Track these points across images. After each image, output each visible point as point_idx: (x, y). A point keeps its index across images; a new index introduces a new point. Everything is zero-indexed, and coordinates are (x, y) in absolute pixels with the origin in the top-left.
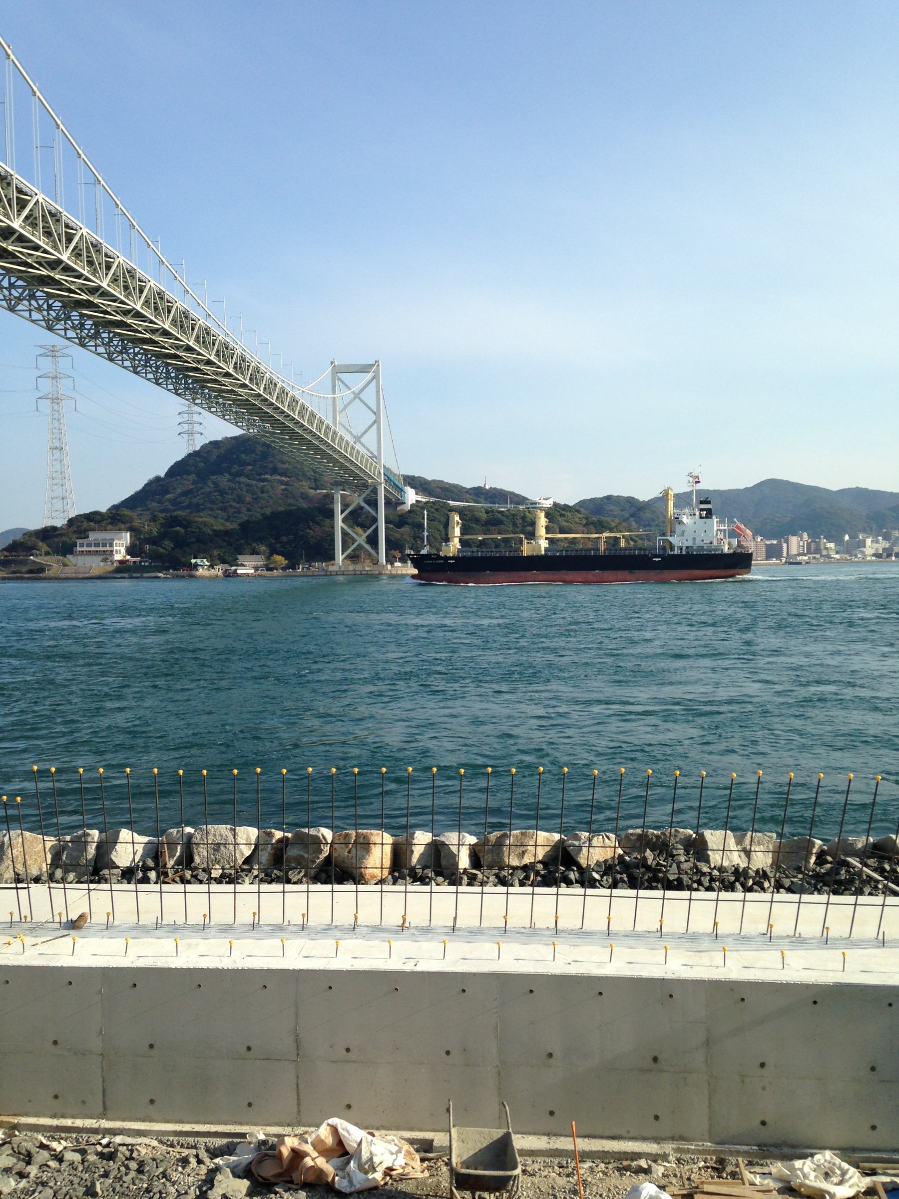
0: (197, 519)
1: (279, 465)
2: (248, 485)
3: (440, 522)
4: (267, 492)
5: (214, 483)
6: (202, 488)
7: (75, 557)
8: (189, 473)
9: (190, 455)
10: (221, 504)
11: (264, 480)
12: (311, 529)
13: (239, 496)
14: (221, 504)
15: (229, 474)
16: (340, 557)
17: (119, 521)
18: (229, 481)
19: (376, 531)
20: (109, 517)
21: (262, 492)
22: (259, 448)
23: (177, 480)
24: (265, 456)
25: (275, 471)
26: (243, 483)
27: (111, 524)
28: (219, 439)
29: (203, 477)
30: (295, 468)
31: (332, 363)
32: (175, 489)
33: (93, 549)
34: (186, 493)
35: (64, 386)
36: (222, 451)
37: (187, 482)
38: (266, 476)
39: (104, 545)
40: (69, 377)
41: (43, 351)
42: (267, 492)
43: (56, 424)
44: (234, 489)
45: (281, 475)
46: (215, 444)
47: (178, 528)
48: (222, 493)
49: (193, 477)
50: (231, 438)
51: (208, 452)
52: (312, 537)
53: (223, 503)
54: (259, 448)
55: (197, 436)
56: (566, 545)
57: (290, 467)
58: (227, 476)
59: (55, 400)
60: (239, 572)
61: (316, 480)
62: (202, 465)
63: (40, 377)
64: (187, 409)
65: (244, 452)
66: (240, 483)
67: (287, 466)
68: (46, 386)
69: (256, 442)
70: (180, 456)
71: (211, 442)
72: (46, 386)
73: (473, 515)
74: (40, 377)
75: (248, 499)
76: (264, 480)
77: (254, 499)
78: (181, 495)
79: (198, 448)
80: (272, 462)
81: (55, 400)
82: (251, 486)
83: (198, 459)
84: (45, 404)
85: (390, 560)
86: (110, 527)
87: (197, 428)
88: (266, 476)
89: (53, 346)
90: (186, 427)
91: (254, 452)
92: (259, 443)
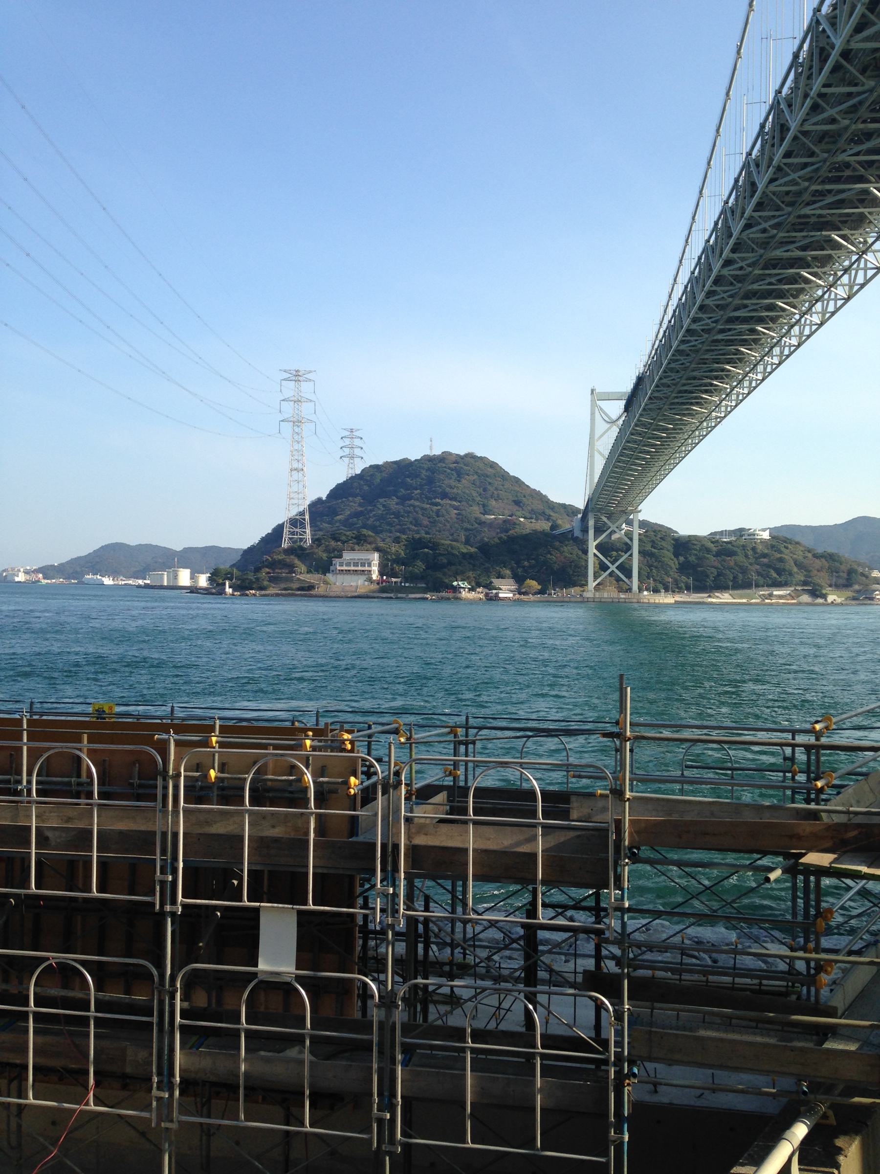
0: (443, 541)
1: (448, 490)
2: (422, 509)
3: (668, 551)
4: (443, 516)
5: (384, 506)
6: (371, 511)
7: (335, 576)
8: (355, 496)
9: (352, 478)
10: (398, 527)
11: (437, 504)
12: (551, 554)
13: (416, 519)
14: (398, 527)
15: (397, 498)
16: (592, 584)
17: (365, 541)
18: (397, 504)
19: (631, 555)
20: (352, 537)
21: (438, 516)
22: (424, 473)
23: (343, 502)
24: (430, 481)
25: (444, 496)
26: (418, 506)
27: (358, 544)
28: (380, 463)
29: (370, 499)
30: (464, 493)
31: (592, 391)
32: (343, 510)
33: (352, 568)
34: (357, 515)
35: (306, 409)
36: (384, 475)
37: (354, 505)
38: (437, 500)
39: (363, 565)
40: (311, 401)
41: (287, 375)
42: (443, 516)
43: (296, 447)
44: (409, 512)
45: (451, 499)
46: (376, 468)
47: (426, 550)
48: (397, 515)
49: (358, 499)
50: (392, 462)
51: (372, 475)
52: (555, 563)
53: (400, 525)
54: (424, 473)
55: (357, 460)
56: (802, 579)
57: (459, 492)
58: (396, 500)
59: (297, 422)
60: (501, 595)
61: (484, 506)
62: (366, 488)
63: (283, 400)
64: (348, 433)
65: (409, 477)
66: (414, 506)
67: (455, 490)
68: (288, 409)
69: (420, 467)
70: (341, 479)
71: (371, 466)
72: (288, 409)
73: (703, 545)
74: (283, 400)
75: (426, 522)
76: (437, 504)
77: (430, 522)
78: (352, 516)
79: (358, 472)
80: (440, 487)
81: (297, 422)
82: (425, 509)
83: (362, 482)
84: (287, 428)
85: (640, 590)
86: (356, 547)
87: (357, 452)
88: (437, 500)
89: (297, 371)
90: (347, 451)
91: (417, 476)
92: (423, 468)
